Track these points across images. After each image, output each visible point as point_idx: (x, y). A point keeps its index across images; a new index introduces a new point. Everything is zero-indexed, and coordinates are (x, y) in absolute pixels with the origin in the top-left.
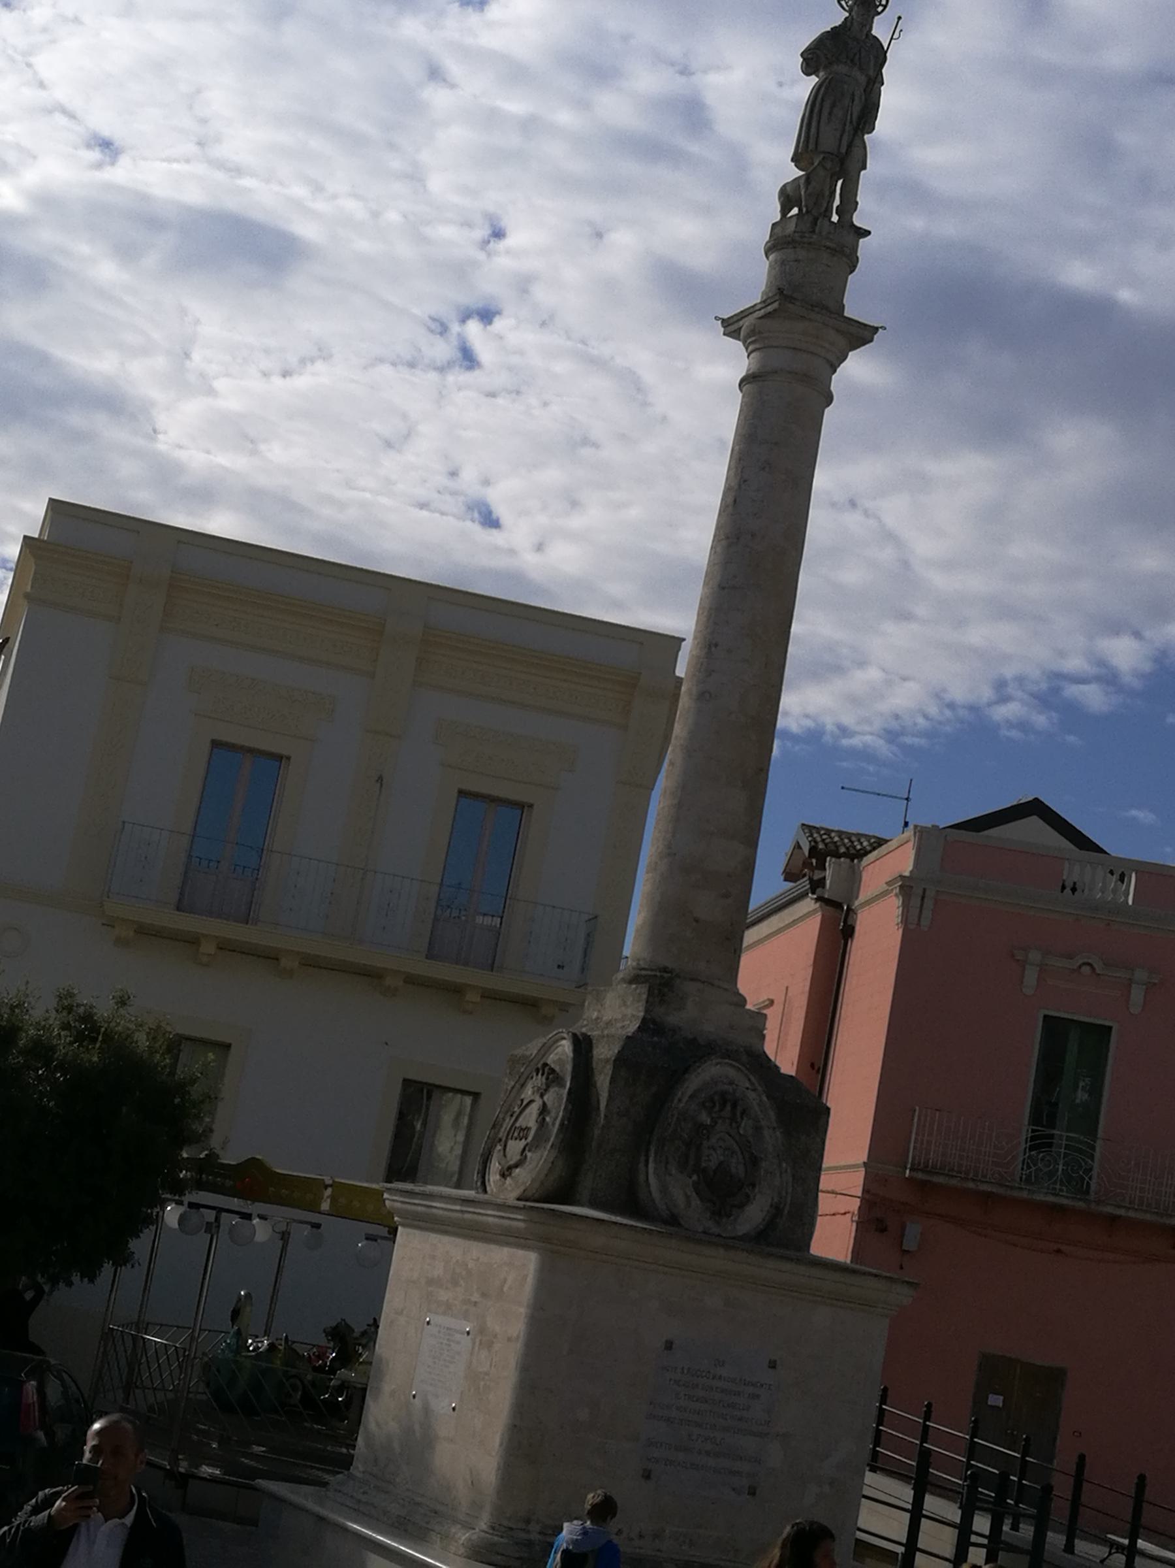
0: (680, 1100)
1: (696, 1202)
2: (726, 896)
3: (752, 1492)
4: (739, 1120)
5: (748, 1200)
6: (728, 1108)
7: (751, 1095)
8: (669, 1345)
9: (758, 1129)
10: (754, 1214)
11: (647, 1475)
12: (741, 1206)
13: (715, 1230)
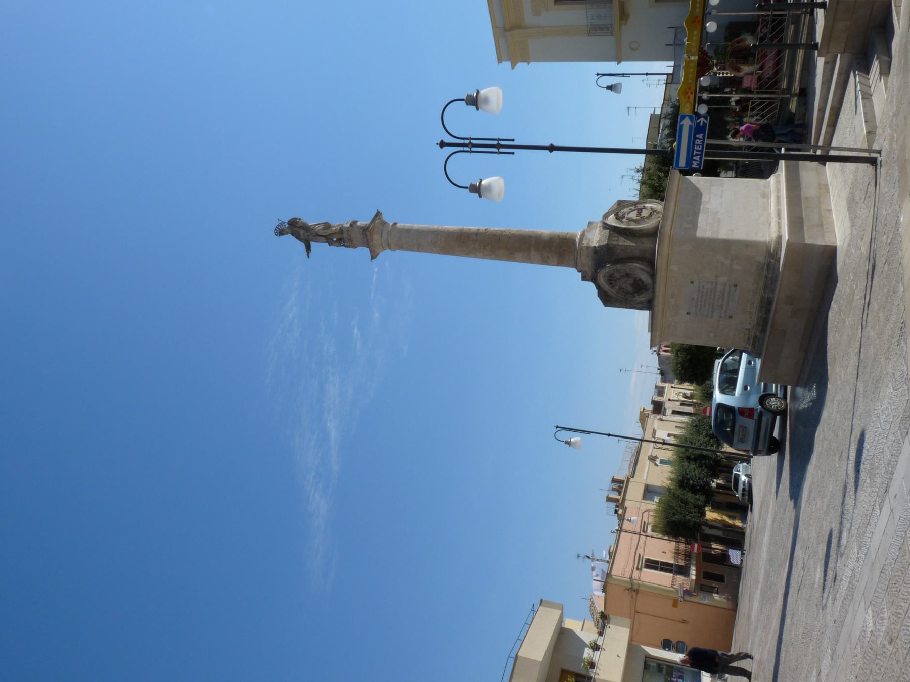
0: (613, 293)
1: (643, 295)
2: (548, 257)
3: (735, 286)
4: (615, 279)
5: (640, 280)
6: (612, 282)
7: (607, 270)
8: (688, 313)
9: (618, 271)
10: (644, 277)
11: (730, 317)
12: (642, 282)
13: (651, 290)
